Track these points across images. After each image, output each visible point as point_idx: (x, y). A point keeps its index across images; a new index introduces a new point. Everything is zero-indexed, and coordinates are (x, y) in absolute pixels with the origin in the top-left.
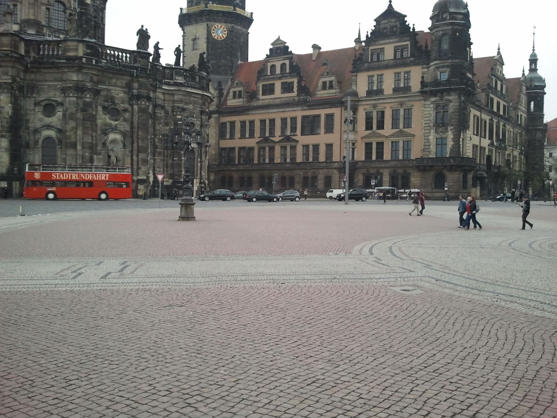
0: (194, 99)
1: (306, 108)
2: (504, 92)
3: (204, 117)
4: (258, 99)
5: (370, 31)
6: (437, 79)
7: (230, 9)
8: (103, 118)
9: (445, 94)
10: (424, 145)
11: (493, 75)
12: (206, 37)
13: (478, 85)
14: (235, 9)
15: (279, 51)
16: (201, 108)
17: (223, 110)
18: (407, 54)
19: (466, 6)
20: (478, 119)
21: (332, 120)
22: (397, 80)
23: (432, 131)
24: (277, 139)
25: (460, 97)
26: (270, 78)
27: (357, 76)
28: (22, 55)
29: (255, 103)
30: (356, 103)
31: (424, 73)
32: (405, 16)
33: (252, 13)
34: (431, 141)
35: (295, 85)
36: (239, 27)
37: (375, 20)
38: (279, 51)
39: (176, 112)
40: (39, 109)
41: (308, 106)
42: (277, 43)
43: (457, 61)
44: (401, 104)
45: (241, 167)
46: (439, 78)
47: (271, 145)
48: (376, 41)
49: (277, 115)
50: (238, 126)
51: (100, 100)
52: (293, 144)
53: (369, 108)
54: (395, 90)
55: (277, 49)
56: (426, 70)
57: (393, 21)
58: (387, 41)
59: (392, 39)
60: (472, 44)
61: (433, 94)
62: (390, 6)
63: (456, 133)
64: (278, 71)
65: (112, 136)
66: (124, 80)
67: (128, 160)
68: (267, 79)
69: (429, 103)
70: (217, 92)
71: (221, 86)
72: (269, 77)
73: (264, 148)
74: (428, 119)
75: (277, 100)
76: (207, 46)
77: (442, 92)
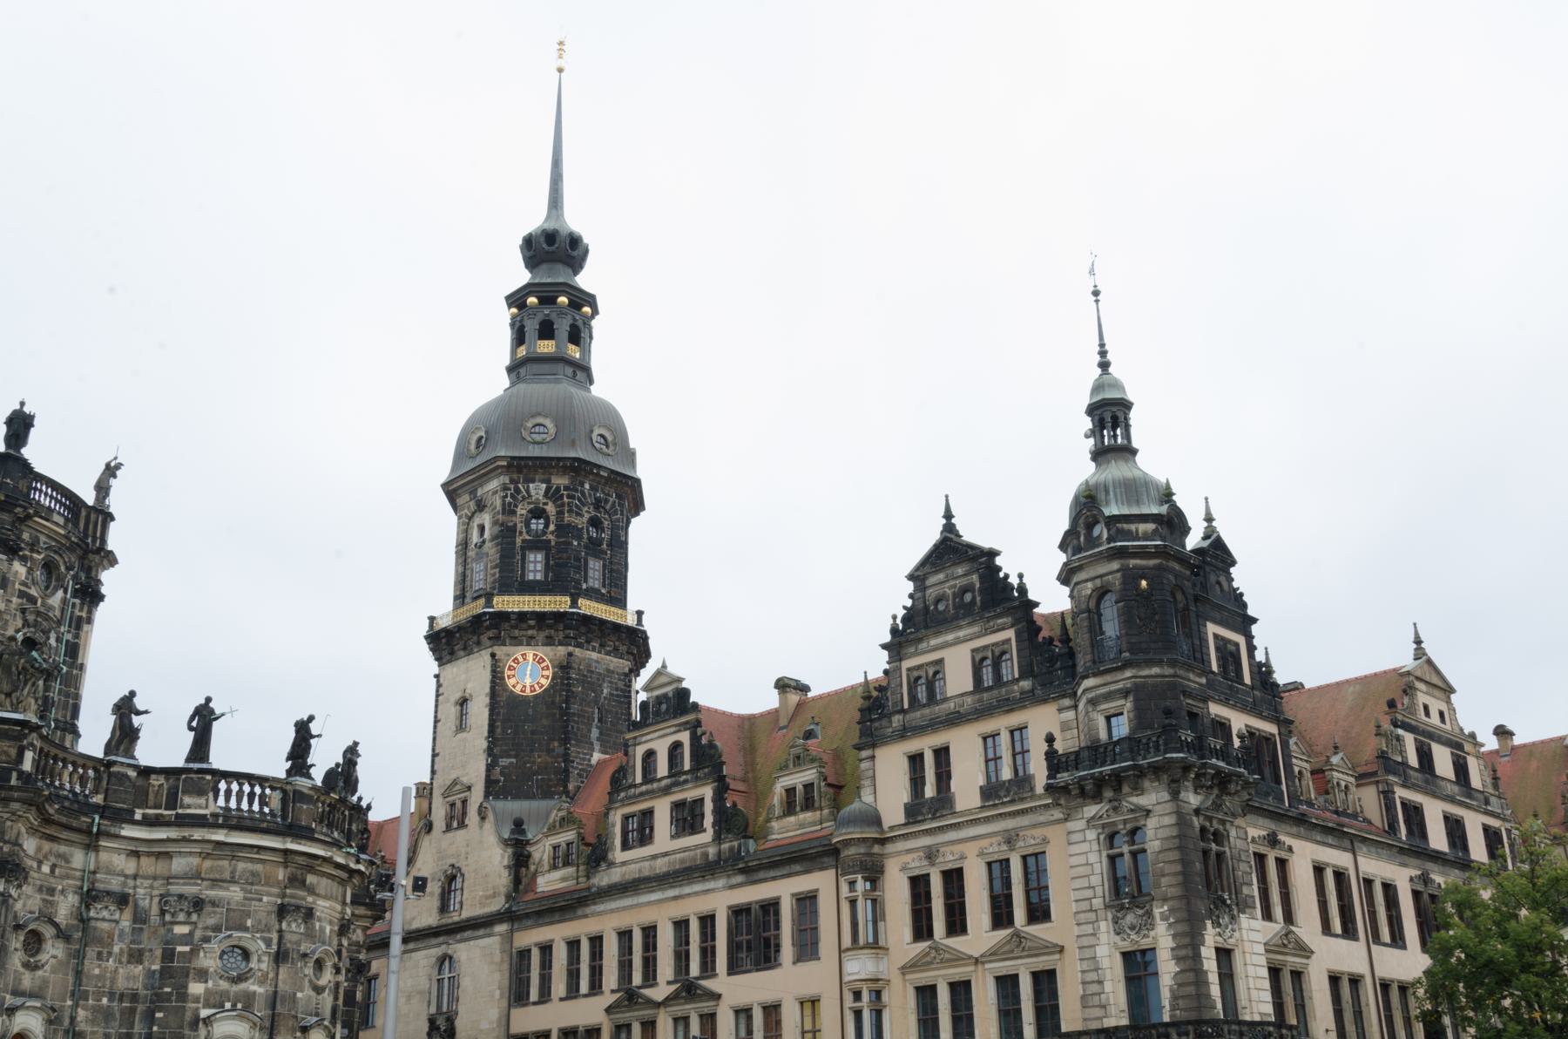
0: (250, 866)
1: (740, 879)
2: (1476, 781)
3: (294, 927)
4: (611, 864)
5: (901, 613)
6: (1098, 740)
7: (561, 603)
9: (1126, 789)
10: (1084, 983)
11: (1396, 726)
12: (487, 690)
13: (1335, 760)
14: (574, 604)
15: (664, 707)
16: (284, 896)
18: (1011, 669)
19: (1167, 496)
20: (1340, 876)
21: (815, 913)
22: (992, 760)
23: (1103, 925)
24: (659, 993)
25: (1175, 795)
26: (642, 794)
27: (873, 757)
29: (604, 878)
30: (876, 849)
31: (1065, 727)
32: (993, 554)
33: (640, 614)
34: (1105, 963)
35: (708, 807)
36: (594, 655)
37: (911, 577)
38: (664, 707)
39: (173, 915)
41: (742, 871)
42: (657, 683)
43: (1155, 670)
44: (1010, 840)
46: (1103, 736)
47: (647, 1013)
48: (920, 640)
49: (661, 910)
50: (560, 956)
52: (706, 1006)
53: (918, 866)
54: (991, 792)
55: (659, 700)
56: (1071, 715)
57: (960, 571)
58: (950, 637)
59: (960, 628)
60: (1254, 620)
61: (1092, 791)
62: (949, 528)
63: (1181, 928)
64: (662, 768)
68: (635, 796)
69: (1081, 824)
70: (510, 850)
71: (523, 832)
72: (638, 791)
73: (628, 1027)
74: (1084, 883)
75: (659, 862)
76: (491, 715)
77: (1117, 781)
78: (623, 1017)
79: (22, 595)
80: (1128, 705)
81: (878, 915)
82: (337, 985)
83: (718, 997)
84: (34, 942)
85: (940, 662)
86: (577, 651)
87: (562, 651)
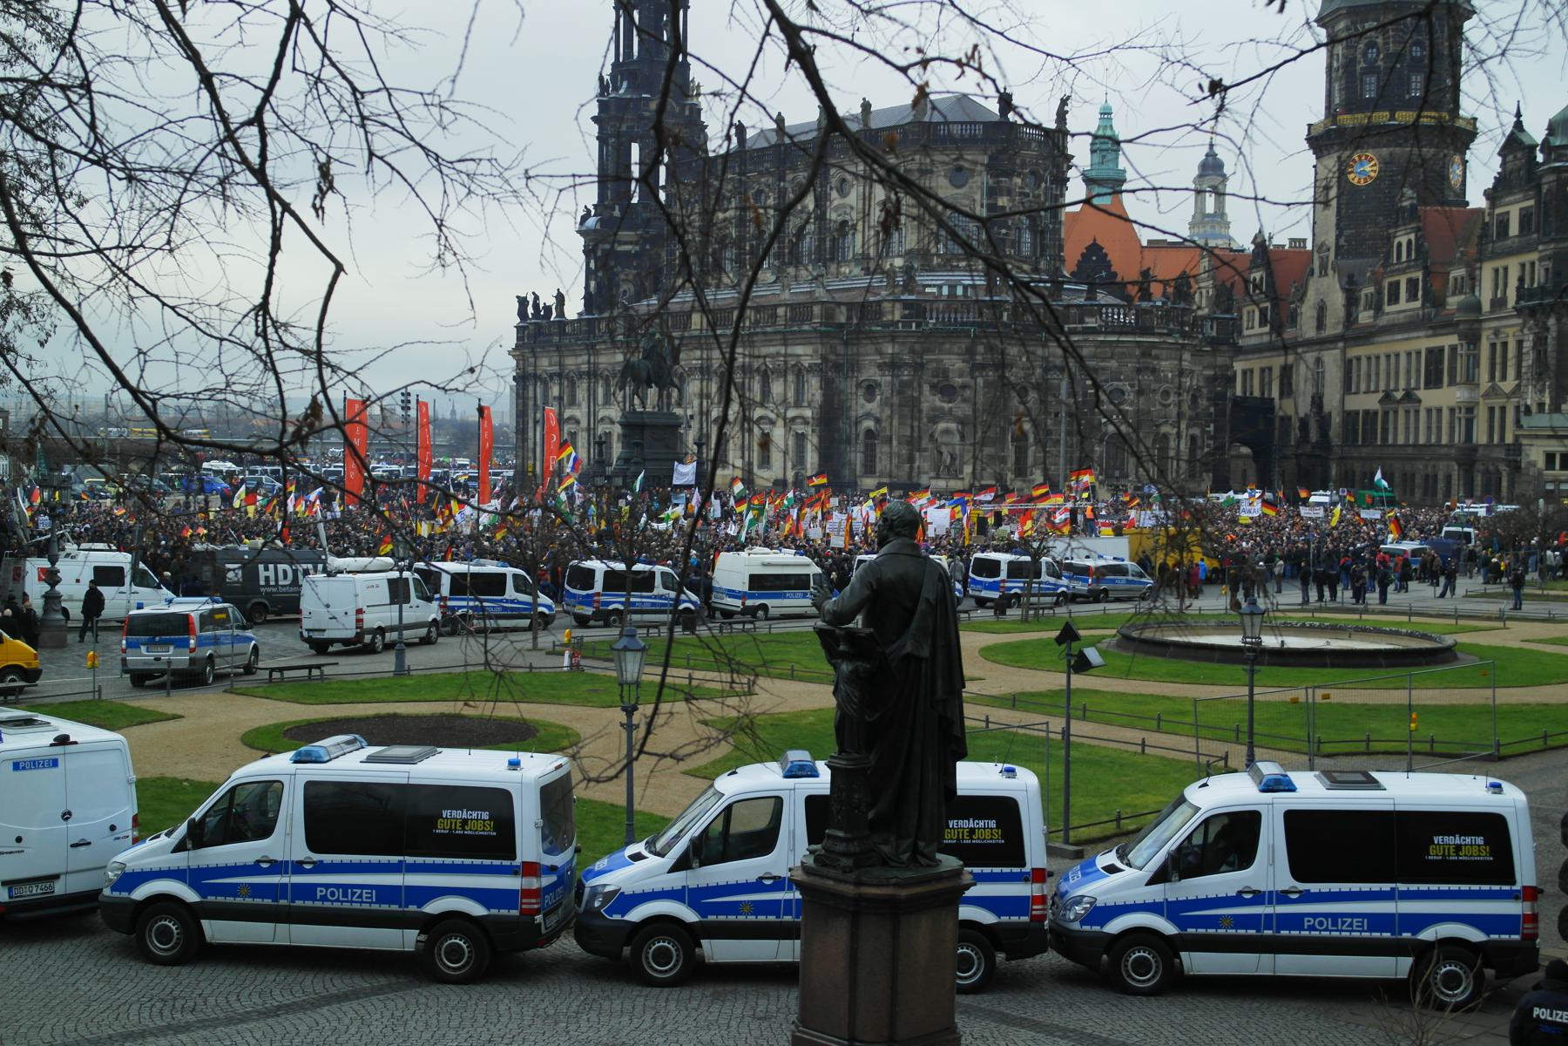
3: (1147, 378)
8: (931, 400)
14: (1392, 117)
17: (1354, 335)
24: (1399, 395)
25: (1559, 320)
28: (841, 326)
29: (1383, 321)
40: (860, 392)
41: (1432, 328)
45: (1365, 451)
51: (927, 376)
57: (1519, 155)
61: (1532, 312)
62: (1519, 125)
64: (1404, 258)
65: (942, 425)
66: (963, 344)
67: (968, 456)
78: (1387, 407)
79: (1021, 194)
80: (1549, 264)
81: (1477, 364)
82: (1180, 402)
83: (1420, 401)
84: (1022, 393)
85: (1508, 213)
86: (1398, 150)
87: (1385, 151)
